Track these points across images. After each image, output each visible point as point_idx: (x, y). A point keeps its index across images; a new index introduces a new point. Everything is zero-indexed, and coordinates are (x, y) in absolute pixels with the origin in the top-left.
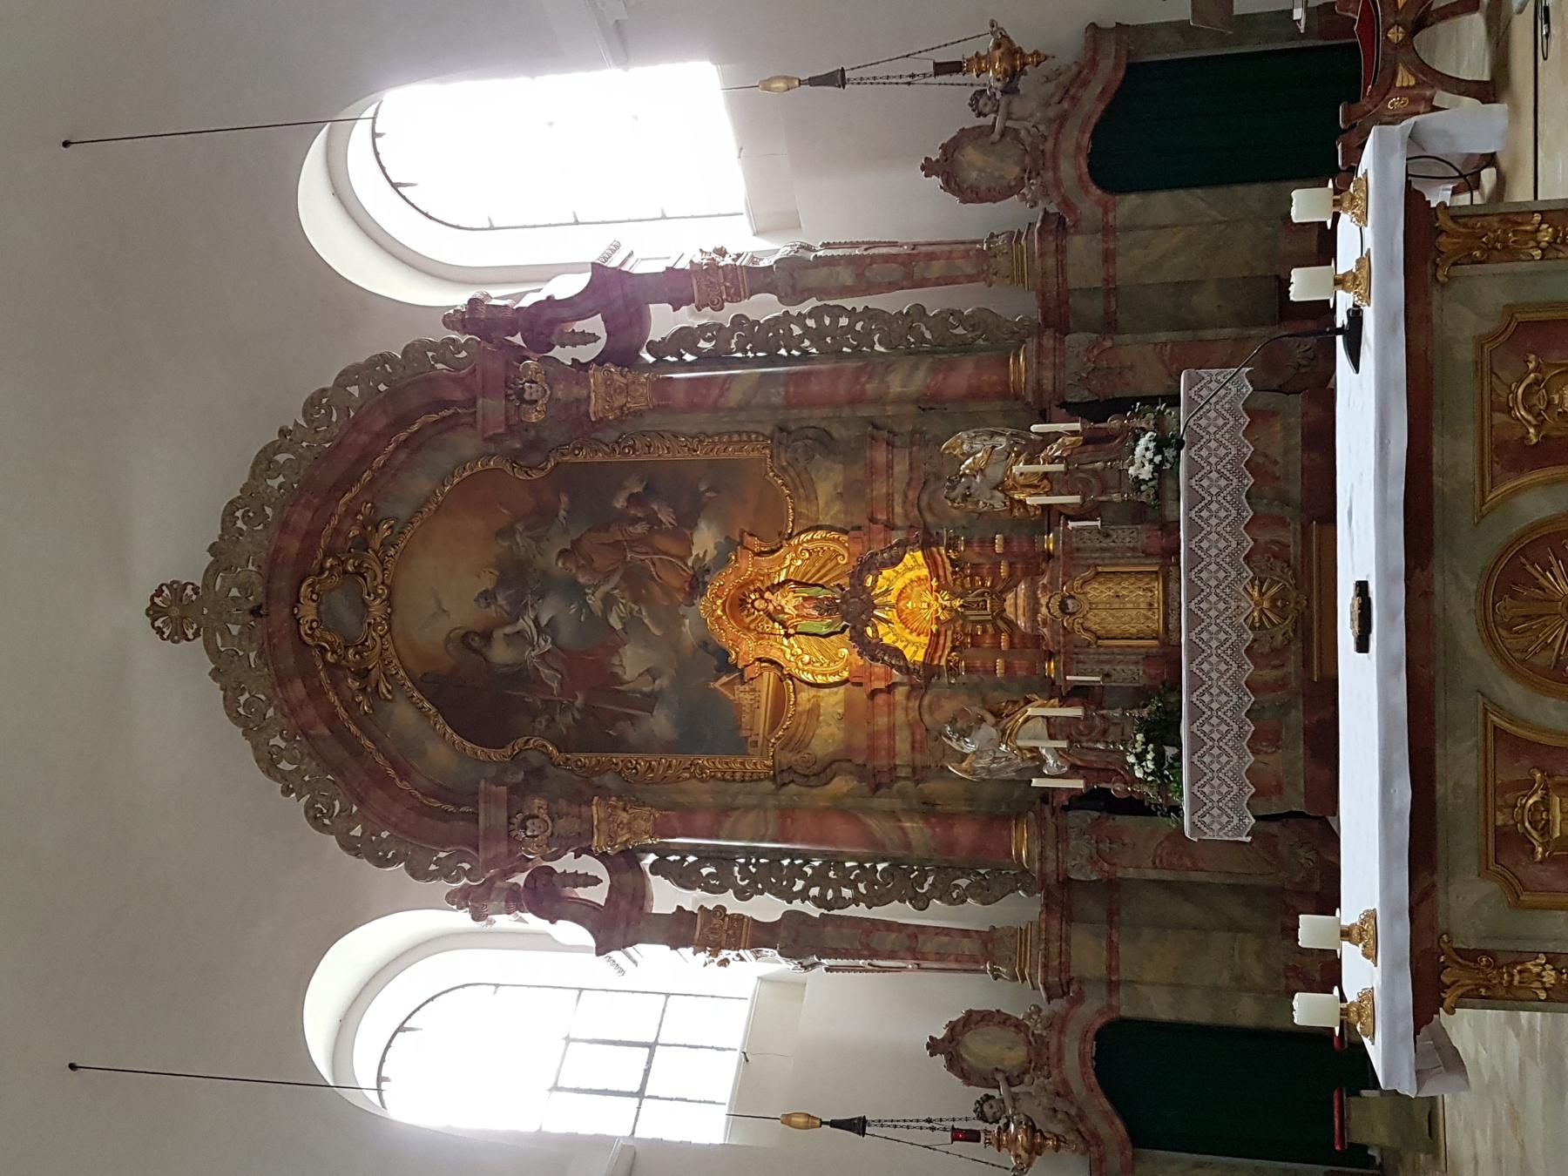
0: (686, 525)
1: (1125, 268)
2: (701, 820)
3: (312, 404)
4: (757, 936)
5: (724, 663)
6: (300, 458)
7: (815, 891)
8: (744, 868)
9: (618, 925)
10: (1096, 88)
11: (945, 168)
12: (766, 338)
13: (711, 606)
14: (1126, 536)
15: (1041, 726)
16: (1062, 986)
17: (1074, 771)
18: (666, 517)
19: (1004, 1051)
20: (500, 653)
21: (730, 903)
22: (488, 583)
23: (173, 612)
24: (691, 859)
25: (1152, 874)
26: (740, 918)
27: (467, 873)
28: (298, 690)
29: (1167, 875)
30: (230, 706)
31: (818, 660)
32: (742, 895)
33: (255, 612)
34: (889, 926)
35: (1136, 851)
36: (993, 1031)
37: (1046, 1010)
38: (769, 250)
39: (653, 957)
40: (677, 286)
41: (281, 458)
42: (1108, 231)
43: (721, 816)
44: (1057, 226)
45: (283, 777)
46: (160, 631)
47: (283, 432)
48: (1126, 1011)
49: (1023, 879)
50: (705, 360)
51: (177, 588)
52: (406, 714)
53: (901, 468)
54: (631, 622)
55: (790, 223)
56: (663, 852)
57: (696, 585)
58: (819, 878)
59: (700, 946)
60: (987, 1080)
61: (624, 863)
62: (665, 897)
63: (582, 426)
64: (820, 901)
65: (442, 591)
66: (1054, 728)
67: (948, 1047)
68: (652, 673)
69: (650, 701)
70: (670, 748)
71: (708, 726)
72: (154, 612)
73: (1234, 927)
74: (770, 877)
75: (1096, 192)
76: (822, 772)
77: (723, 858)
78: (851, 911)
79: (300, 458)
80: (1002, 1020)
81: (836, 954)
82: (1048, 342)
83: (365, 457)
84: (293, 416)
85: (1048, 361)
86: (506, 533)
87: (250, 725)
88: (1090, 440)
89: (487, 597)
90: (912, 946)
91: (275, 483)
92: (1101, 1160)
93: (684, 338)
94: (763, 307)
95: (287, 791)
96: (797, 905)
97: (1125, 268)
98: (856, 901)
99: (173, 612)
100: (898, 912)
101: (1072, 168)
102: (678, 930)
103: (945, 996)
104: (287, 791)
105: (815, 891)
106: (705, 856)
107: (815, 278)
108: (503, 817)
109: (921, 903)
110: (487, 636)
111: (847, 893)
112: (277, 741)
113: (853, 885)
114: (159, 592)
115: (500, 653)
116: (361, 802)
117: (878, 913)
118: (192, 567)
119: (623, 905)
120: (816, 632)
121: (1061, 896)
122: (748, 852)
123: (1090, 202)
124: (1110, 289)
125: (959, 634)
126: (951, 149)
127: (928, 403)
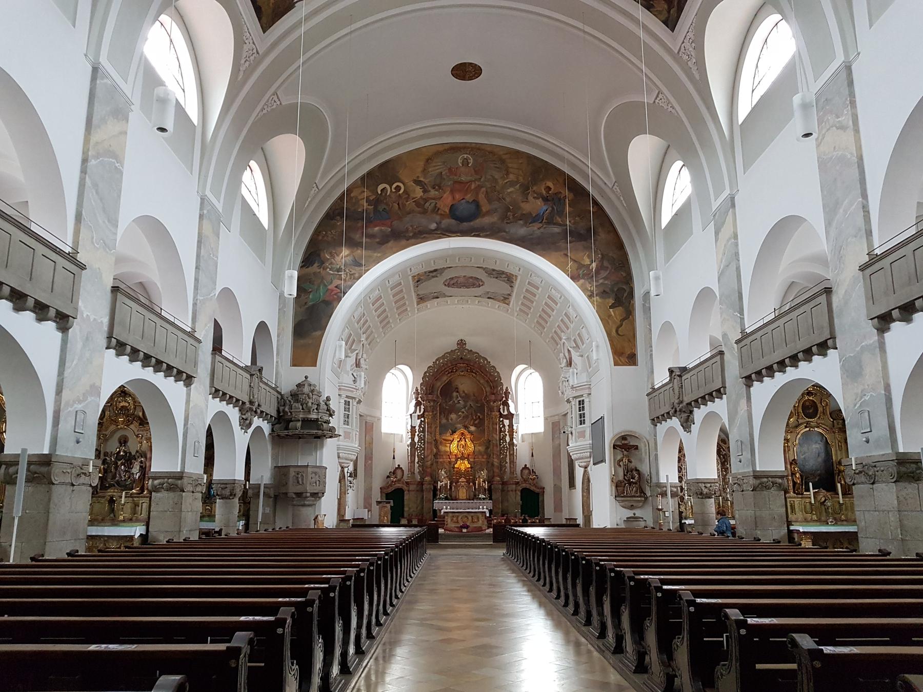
0: (475, 425)
4: (413, 439)
5: (454, 432)
13: (463, 430)
20: (455, 394)
31: (454, 447)
43: (430, 433)
52: (445, 379)
54: (460, 416)
57: (466, 427)
63: (491, 410)
65: (465, 384)
69: (447, 419)
71: (444, 429)
76: (437, 448)
77: (423, 431)
106: (424, 428)
115: (455, 394)
120: (458, 446)
125: (459, 474)
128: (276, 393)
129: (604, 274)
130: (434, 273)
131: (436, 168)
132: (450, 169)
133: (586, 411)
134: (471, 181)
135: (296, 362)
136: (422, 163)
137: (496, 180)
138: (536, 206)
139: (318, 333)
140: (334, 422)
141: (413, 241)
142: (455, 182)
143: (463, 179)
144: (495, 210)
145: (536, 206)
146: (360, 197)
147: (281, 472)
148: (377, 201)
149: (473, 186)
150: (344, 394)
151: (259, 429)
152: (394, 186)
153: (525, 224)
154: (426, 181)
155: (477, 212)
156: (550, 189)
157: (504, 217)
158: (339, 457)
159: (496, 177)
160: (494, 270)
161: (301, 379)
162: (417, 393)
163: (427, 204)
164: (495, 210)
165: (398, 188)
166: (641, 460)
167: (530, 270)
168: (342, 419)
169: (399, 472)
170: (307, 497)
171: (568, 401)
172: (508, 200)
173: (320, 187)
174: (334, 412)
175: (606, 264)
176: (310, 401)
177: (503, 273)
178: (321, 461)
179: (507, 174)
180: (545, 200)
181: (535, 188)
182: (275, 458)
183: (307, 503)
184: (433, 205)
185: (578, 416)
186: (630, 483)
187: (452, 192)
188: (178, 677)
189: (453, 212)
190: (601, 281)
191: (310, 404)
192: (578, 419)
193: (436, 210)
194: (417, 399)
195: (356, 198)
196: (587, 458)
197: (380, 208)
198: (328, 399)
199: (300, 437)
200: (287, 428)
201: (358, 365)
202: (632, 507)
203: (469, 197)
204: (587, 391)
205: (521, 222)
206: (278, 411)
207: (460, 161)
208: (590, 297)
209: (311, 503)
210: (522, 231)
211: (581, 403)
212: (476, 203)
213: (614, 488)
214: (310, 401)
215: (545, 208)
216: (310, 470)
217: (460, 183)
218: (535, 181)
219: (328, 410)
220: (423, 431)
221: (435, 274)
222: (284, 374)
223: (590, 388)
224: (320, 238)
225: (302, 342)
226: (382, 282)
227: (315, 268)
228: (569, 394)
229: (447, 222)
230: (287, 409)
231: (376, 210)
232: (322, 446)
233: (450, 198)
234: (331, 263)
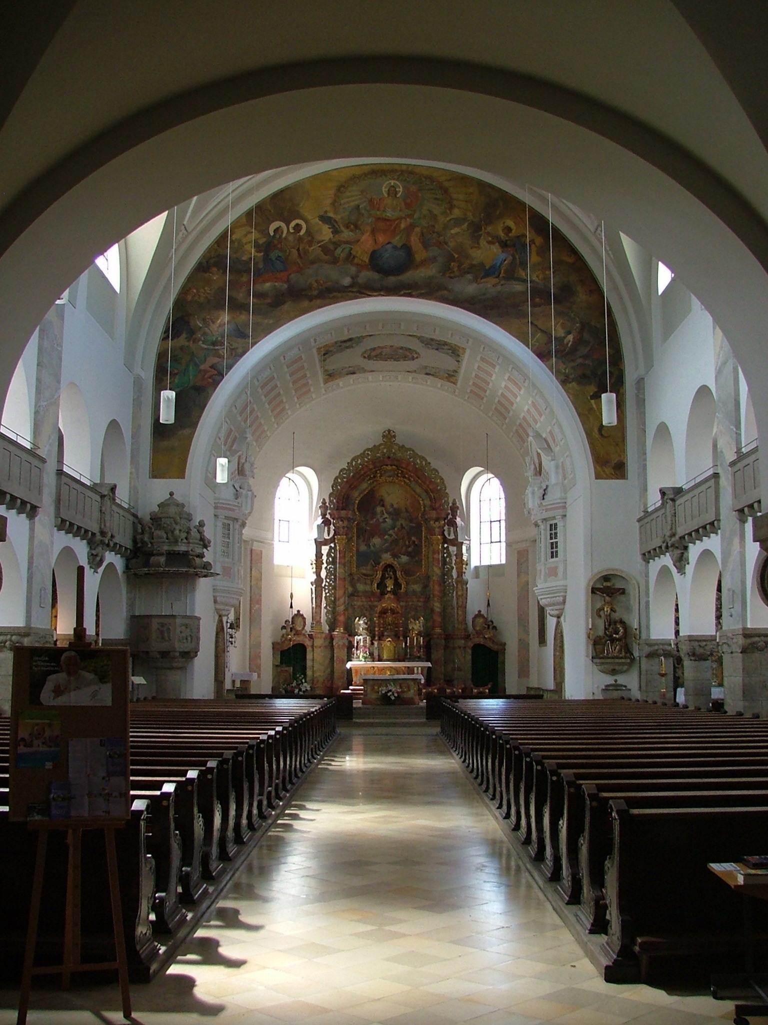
0: (408, 554)
1: (458, 651)
2: (343, 561)
4: (318, 573)
10: (491, 645)
11: (479, 615)
18: (410, 549)
20: (379, 509)
21: (325, 565)
22: (395, 506)
23: (389, 435)
28: (371, 467)
30: (368, 450)
33: (389, 458)
38: (468, 576)
40: (460, 554)
44: (467, 637)
49: (332, 629)
50: (444, 559)
51: (394, 436)
53: (420, 604)
54: (386, 540)
56: (335, 548)
58: (330, 585)
60: (293, 623)
61: (332, 540)
62: (325, 550)
63: (431, 531)
65: (394, 495)
67: (299, 614)
68: (374, 545)
69: (368, 546)
70: (357, 550)
72: (389, 431)
80: (304, 626)
83: (425, 483)
84: (434, 464)
86: (407, 511)
87: (362, 455)
89: (392, 506)
90: (319, 605)
93: (449, 555)
94: (454, 573)
97: (458, 651)
100: (324, 604)
102: (319, 555)
103: (307, 612)
106: (334, 558)
107: (459, 586)
109: (325, 608)
110: (383, 506)
115: (379, 509)
118: (399, 440)
122: (335, 569)
123: (470, 644)
124: (454, 648)
126: (483, 616)
127: (432, 611)
128: (132, 518)
129: (584, 350)
130: (348, 343)
131: (352, 198)
132: (371, 201)
133: (560, 539)
134: (401, 218)
135: (157, 472)
136: (332, 192)
137: (434, 217)
138: (488, 253)
139: (186, 432)
140: (208, 556)
141: (319, 301)
142: (379, 219)
143: (389, 214)
144: (434, 259)
145: (488, 253)
146: (244, 241)
147: (138, 624)
148: (268, 247)
149: (403, 226)
150: (222, 513)
151: (111, 565)
152: (293, 224)
153: (476, 279)
154: (338, 217)
155: (408, 261)
156: (508, 230)
157: (446, 269)
158: (215, 602)
159: (436, 212)
160: (432, 340)
161: (163, 496)
162: (324, 507)
163: (339, 250)
164: (434, 259)
165: (298, 228)
166: (628, 609)
167: (481, 342)
168: (219, 549)
169: (299, 621)
170: (174, 658)
171: (536, 525)
172: (452, 244)
173: (189, 230)
174: (209, 542)
175: (586, 336)
176: (178, 527)
177: (445, 344)
178: (193, 610)
179: (451, 207)
180: (504, 245)
181: (489, 229)
182: (131, 605)
183: (175, 665)
184: (346, 251)
185: (549, 546)
186: (613, 641)
187: (373, 232)
189: (374, 261)
190: (580, 361)
191: (177, 532)
192: (549, 551)
193: (350, 258)
195: (239, 241)
196: (558, 604)
197: (274, 255)
198: (202, 524)
199: (163, 575)
200: (147, 564)
202: (613, 672)
203: (397, 241)
204: (561, 511)
205: (469, 276)
206: (135, 541)
207: (384, 190)
208: (565, 381)
209: (180, 665)
210: (470, 288)
211: (553, 527)
212: (407, 248)
213: (591, 647)
214: (178, 527)
215: (502, 256)
216: (178, 621)
217: (385, 220)
218: (489, 220)
219: (202, 539)
220: (334, 562)
221: (348, 344)
222: (141, 491)
223: (564, 507)
224: (189, 298)
225: (165, 444)
226: (275, 360)
227: (182, 340)
228: (537, 515)
229: (367, 275)
230: (146, 539)
231: (267, 259)
232: (194, 589)
233: (371, 242)
234: (205, 334)
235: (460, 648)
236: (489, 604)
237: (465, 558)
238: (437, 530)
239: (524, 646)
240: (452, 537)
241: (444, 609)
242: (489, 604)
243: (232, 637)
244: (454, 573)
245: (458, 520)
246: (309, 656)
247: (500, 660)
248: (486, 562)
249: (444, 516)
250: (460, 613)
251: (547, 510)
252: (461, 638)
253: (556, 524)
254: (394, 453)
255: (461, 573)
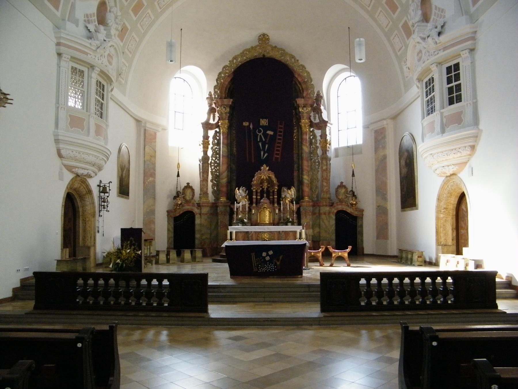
3: (303, 66)
4: (205, 152)
6: (293, 64)
7: (213, 161)
8: (216, 148)
9: (207, 126)
11: (342, 186)
12: (313, 152)
14: (277, 217)
15: (244, 203)
16: (199, 205)
17: (237, 209)
19: (188, 196)
21: (210, 146)
23: (264, 38)
24: (218, 138)
25: (219, 221)
26: (208, 148)
27: (215, 97)
29: (219, 224)
30: (246, 50)
32: (212, 148)
34: (208, 175)
35: (224, 219)
36: (191, 194)
37: (195, 203)
38: (331, 153)
39: (201, 132)
40: (324, 136)
41: (293, 60)
42: (329, 213)
45: (233, 61)
46: (260, 36)
47: (298, 60)
48: (196, 216)
49: (217, 199)
51: (268, 39)
55: (337, 156)
56: (219, 132)
58: (215, 162)
59: (203, 141)
61: (217, 126)
64: (211, 162)
66: (244, 206)
67: (188, 186)
72: (264, 35)
73: (211, 234)
74: (216, 153)
75: (335, 211)
77: (218, 144)
78: (210, 168)
79: (293, 64)
81: (203, 166)
82: (311, 204)
84: (301, 62)
85: (308, 204)
87: (242, 54)
88: (293, 211)
91: (288, 59)
92: (172, 212)
93: (315, 136)
94: (319, 152)
95: (230, 61)
96: (210, 158)
98: (212, 169)
99: (264, 38)
100: (210, 177)
101: (340, 207)
102: (206, 137)
103: (196, 185)
104: (230, 61)
105: (213, 161)
106: (219, 141)
107: (324, 162)
108: (226, 103)
109: (212, 181)
111: (213, 167)
112: (239, 59)
113: (214, 169)
114: (268, 36)
116: (228, 76)
117: (210, 173)
119: (209, 126)
121: (214, 206)
122: (220, 149)
126: (345, 187)
158: (60, 155)
162: (210, 98)
188: (31, 361)
192: (446, 97)
194: (210, 105)
201: (102, 21)
220: (218, 144)
223: (473, 38)
235: (325, 214)
236: (353, 175)
237: (328, 138)
238: (305, 114)
239: (382, 212)
240: (317, 121)
241: (311, 182)
242: (353, 175)
243: (104, 202)
244: (319, 152)
245: (322, 108)
246: (198, 221)
247: (359, 224)
248: (343, 144)
249: (310, 102)
250: (325, 184)
251: (445, 49)
252: (326, 206)
253: (457, 66)
254: (269, 53)
255: (325, 150)
